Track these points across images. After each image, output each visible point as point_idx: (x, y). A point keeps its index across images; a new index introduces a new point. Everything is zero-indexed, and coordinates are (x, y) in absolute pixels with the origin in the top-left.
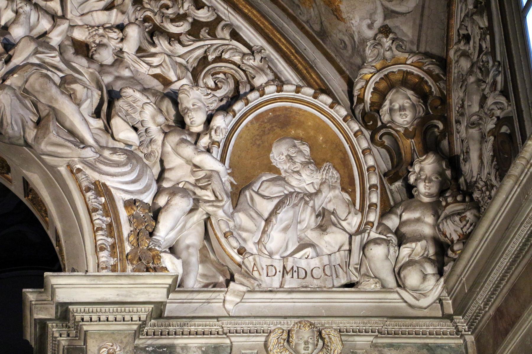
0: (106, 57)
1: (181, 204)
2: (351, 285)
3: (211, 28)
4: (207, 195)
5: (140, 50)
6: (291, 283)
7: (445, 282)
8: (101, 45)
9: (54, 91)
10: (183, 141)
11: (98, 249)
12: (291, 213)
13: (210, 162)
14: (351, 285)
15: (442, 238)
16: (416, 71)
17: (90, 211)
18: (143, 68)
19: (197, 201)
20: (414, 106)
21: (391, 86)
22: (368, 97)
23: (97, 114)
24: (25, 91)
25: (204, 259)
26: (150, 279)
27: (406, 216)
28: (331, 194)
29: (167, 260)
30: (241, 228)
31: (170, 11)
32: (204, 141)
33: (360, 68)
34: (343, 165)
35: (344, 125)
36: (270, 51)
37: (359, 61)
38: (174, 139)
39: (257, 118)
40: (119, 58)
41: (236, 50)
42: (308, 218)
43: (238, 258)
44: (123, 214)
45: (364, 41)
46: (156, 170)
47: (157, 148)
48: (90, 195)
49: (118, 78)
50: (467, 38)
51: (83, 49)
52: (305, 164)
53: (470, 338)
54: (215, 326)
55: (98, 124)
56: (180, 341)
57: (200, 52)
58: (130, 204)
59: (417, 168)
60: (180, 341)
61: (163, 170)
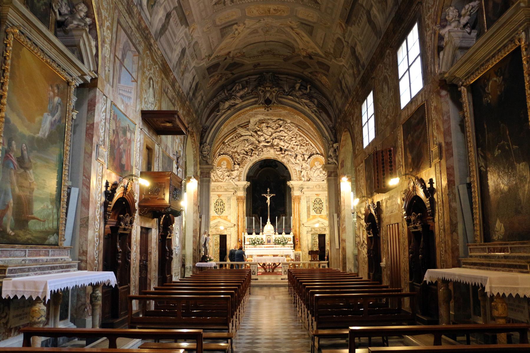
29: (303, 178)
42: (319, 172)
51: (293, 148)
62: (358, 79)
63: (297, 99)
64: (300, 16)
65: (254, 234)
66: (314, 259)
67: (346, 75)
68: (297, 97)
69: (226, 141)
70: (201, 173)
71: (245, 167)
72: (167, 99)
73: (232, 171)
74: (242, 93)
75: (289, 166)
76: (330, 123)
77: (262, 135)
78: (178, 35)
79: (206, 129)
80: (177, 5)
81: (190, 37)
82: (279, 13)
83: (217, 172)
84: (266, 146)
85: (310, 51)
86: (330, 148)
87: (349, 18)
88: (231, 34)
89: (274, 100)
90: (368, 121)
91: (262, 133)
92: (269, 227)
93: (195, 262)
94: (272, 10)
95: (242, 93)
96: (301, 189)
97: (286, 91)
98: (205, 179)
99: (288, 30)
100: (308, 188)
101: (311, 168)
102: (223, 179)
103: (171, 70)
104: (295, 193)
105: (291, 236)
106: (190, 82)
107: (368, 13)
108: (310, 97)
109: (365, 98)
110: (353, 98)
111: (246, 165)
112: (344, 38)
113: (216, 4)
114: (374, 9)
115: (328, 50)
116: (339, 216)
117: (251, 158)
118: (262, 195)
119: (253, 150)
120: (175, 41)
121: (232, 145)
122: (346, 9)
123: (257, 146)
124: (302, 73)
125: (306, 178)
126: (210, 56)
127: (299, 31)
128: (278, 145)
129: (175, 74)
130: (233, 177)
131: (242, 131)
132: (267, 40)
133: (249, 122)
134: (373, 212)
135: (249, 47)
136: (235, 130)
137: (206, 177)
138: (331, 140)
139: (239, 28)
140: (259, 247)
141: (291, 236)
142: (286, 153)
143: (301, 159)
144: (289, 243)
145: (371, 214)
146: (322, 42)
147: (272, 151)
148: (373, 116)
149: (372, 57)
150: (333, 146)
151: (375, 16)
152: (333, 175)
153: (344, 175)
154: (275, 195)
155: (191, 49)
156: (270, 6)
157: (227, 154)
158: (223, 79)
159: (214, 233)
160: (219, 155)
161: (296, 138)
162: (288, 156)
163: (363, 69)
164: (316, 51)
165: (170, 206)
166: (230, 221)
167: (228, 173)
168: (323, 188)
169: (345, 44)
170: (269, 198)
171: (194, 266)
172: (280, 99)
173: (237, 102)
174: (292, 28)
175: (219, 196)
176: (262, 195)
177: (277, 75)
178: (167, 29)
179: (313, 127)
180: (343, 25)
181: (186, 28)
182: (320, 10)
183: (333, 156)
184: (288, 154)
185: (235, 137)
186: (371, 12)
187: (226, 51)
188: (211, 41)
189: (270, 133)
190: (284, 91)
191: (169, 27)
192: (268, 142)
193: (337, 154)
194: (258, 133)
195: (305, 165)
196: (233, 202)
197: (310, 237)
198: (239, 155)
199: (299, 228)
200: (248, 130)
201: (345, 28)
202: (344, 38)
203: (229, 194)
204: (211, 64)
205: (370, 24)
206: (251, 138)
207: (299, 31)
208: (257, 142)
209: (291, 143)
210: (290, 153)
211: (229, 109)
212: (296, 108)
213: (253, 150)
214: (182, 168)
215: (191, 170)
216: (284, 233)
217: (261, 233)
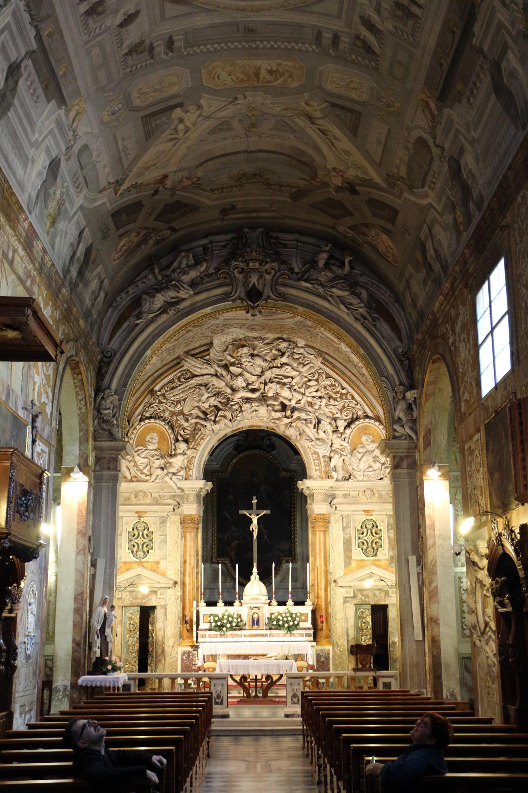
0: (317, 407)
2: (381, 479)
3: (346, 395)
4: (344, 453)
6: (365, 479)
8: (315, 404)
11: (316, 471)
14: (381, 479)
17: (314, 460)
19: (341, 454)
23: (315, 428)
25: (343, 469)
26: (329, 481)
29: (334, 474)
30: (353, 462)
32: (343, 436)
36: (363, 403)
38: (335, 435)
42: (371, 459)
44: (322, 460)
47: (330, 437)
51: (310, 404)
56: (336, 493)
57: (343, 404)
58: (324, 457)
60: (336, 493)
61: (332, 444)
62: (466, 236)
63: (321, 290)
64: (330, 87)
65: (221, 603)
66: (364, 666)
67: (437, 228)
68: (321, 285)
70: (98, 459)
71: (200, 448)
72: (13, 277)
73: (171, 456)
74: (193, 274)
75: (302, 445)
76: (398, 343)
77: (240, 375)
78: (39, 124)
79: (111, 358)
80: (35, 46)
81: (71, 133)
82: (281, 80)
83: (137, 458)
84: (248, 400)
85: (351, 173)
86: (398, 403)
87: (446, 88)
88: (169, 131)
89: (267, 292)
90: (491, 332)
91: (240, 370)
92: (255, 588)
93: (76, 673)
94: (263, 72)
95: (193, 274)
96: (331, 498)
97: (297, 270)
98: (106, 473)
99: (301, 122)
100: (345, 496)
101: (353, 450)
102: (151, 475)
103: (21, 208)
104: (317, 508)
105: (307, 609)
106: (72, 244)
107: (496, 68)
108: (352, 285)
109: (484, 276)
110: (455, 280)
111: (203, 443)
112: (434, 137)
113: (130, 53)
114: (510, 56)
115: (396, 171)
116: (420, 562)
117: (216, 427)
118: (241, 512)
119: (218, 409)
120: (33, 140)
121: (172, 396)
122: (441, 65)
123: (229, 400)
124: (333, 228)
125: (341, 474)
126: (119, 183)
127: (325, 124)
128: (276, 397)
129: (32, 219)
130: (174, 470)
131: (193, 365)
132: (251, 149)
133: (211, 343)
134: (510, 549)
135: (211, 163)
137: (109, 468)
138: (401, 384)
139: (186, 116)
140: (233, 636)
141: (307, 609)
142: (296, 414)
143: (329, 429)
144: (302, 625)
145: (505, 556)
146: (380, 150)
147: (263, 410)
148: (506, 318)
149: (504, 177)
150: (404, 397)
151: (513, 74)
152: (405, 464)
153: (431, 463)
154: (269, 512)
155: (73, 162)
156: (259, 63)
157: (159, 418)
158: (151, 242)
159: (128, 603)
160: (141, 420)
161: (317, 380)
162: (298, 423)
163: (480, 209)
164: (366, 173)
165: (9, 534)
166: (164, 575)
167: (162, 462)
168: (380, 496)
169: (435, 151)
170: (255, 520)
171: (74, 686)
172: (283, 289)
173: (182, 294)
174: (311, 119)
175: (140, 514)
176: (241, 512)
177: (275, 235)
178: (10, 105)
179: (357, 353)
180: (432, 105)
181: (59, 108)
182: (376, 69)
183: (404, 419)
184: (299, 418)
185: (179, 378)
186: (504, 65)
187: (156, 174)
188: (121, 147)
189: (259, 370)
190: (291, 270)
191: (16, 101)
192: (254, 391)
193: (415, 415)
194: (232, 369)
195: (338, 443)
196: (173, 529)
197: (351, 612)
198: (187, 420)
199: (326, 590)
200: (208, 362)
201: (436, 112)
202: (434, 137)
203: (163, 511)
204: (121, 202)
205: (498, 97)
206: (215, 381)
207: (325, 124)
208: (229, 391)
209: (307, 392)
210: (303, 416)
211: (164, 310)
212: (318, 310)
213: (218, 409)
214: (47, 442)
215: (72, 452)
216: (290, 602)
217: (237, 603)
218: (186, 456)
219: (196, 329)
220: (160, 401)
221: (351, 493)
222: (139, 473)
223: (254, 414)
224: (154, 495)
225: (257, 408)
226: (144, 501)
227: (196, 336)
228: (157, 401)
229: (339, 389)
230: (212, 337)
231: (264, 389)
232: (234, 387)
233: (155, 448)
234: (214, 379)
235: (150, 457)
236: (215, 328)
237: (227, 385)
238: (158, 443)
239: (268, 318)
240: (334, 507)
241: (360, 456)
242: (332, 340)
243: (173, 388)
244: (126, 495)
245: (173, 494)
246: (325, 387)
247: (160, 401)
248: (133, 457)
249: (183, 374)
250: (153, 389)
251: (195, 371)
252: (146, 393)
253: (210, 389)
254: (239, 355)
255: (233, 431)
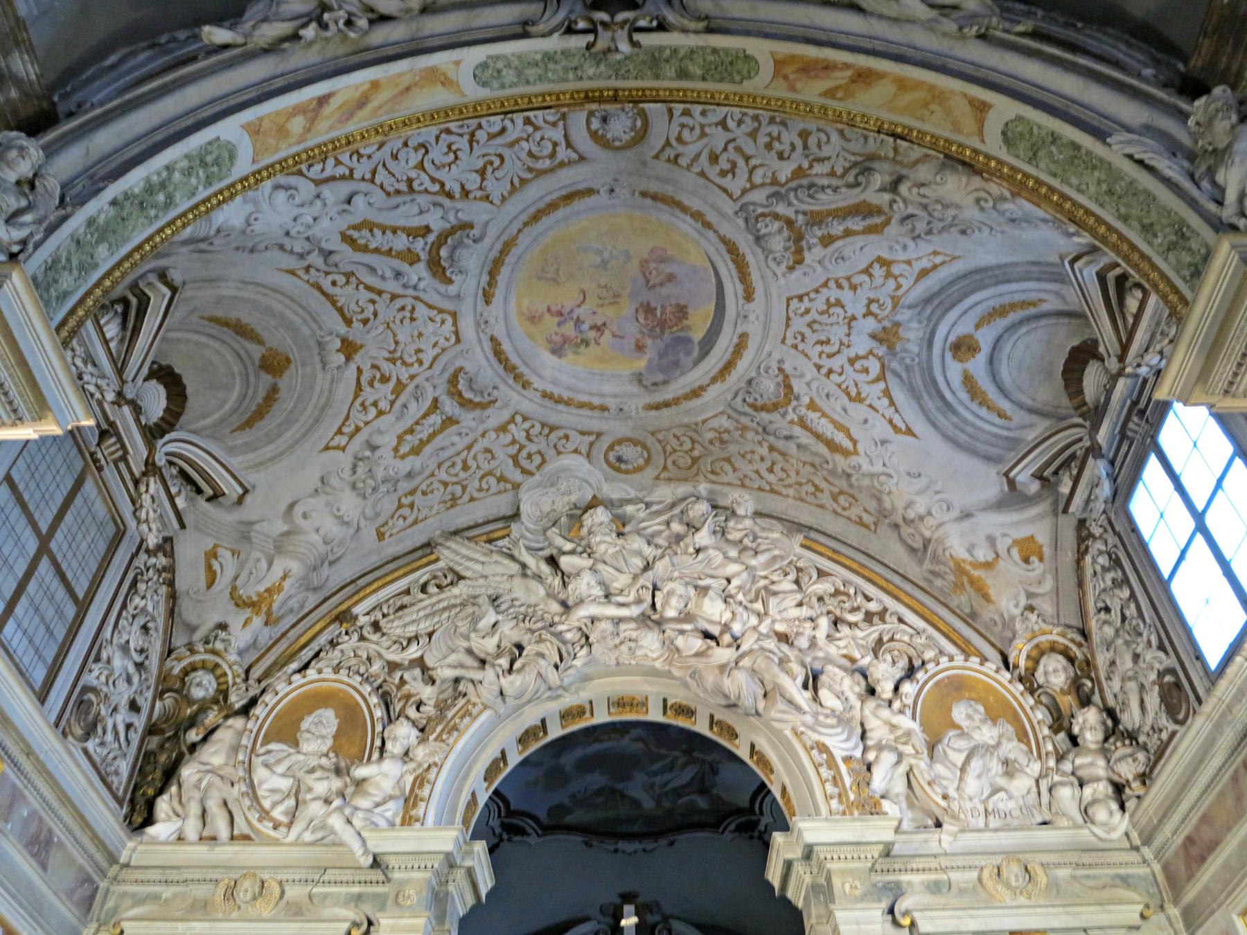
0: (803, 643)
1: (888, 758)
2: (1045, 823)
3: (882, 614)
5: (828, 636)
7: (1132, 816)
9: (776, 669)
10: (879, 706)
11: (828, 798)
12: (980, 763)
13: (905, 722)
14: (1045, 823)
15: (1116, 778)
16: (1061, 640)
17: (817, 767)
18: (832, 650)
20: (1065, 669)
21: (1042, 654)
22: (1022, 663)
24: (754, 671)
25: (911, 806)
26: (876, 821)
27: (1078, 761)
28: (1010, 746)
30: (939, 777)
31: (847, 605)
32: (897, 705)
33: (1011, 641)
34: (1015, 719)
35: (1010, 687)
36: (931, 630)
37: (1010, 634)
38: (871, 704)
39: (936, 684)
40: (813, 643)
41: (905, 632)
42: (996, 767)
43: (943, 803)
44: (843, 768)
45: (1013, 619)
46: (859, 730)
48: (815, 753)
49: (815, 659)
50: (1107, 610)
51: (783, 638)
52: (983, 721)
53: (1157, 867)
54: (933, 863)
55: (808, 694)
56: (905, 878)
57: (875, 636)
58: (848, 759)
59: (1080, 720)
60: (905, 878)
69: (357, 610)
71: (462, 743)
83: (260, 773)
100: (935, 888)
102: (290, 825)
111: (471, 730)
121: (396, 627)
128: (687, 617)
133: (516, 516)
136: (428, 546)
167: (337, 783)
185: (424, 589)
189: (638, 563)
194: (564, 561)
208: (555, 607)
218: (412, 765)
219: (468, 419)
220: (362, 638)
221: (955, 876)
222: (254, 816)
223: (624, 648)
224: (292, 892)
225: (634, 634)
226: (252, 912)
227: (471, 463)
228: (355, 637)
229: (860, 599)
230: (516, 487)
231: (653, 605)
232: (570, 603)
233: (324, 749)
234: (518, 581)
235: (300, 774)
236: (521, 436)
237: (550, 595)
238: (335, 737)
239: (659, 397)
240: (906, 922)
241: (959, 759)
242: (832, 446)
243: (402, 607)
244: (200, 891)
245: (356, 889)
246: (820, 599)
247: (362, 638)
248: (249, 770)
249: (435, 577)
250: (349, 609)
251: (468, 568)
252: (327, 619)
253: (503, 607)
254: (584, 531)
255: (566, 715)
